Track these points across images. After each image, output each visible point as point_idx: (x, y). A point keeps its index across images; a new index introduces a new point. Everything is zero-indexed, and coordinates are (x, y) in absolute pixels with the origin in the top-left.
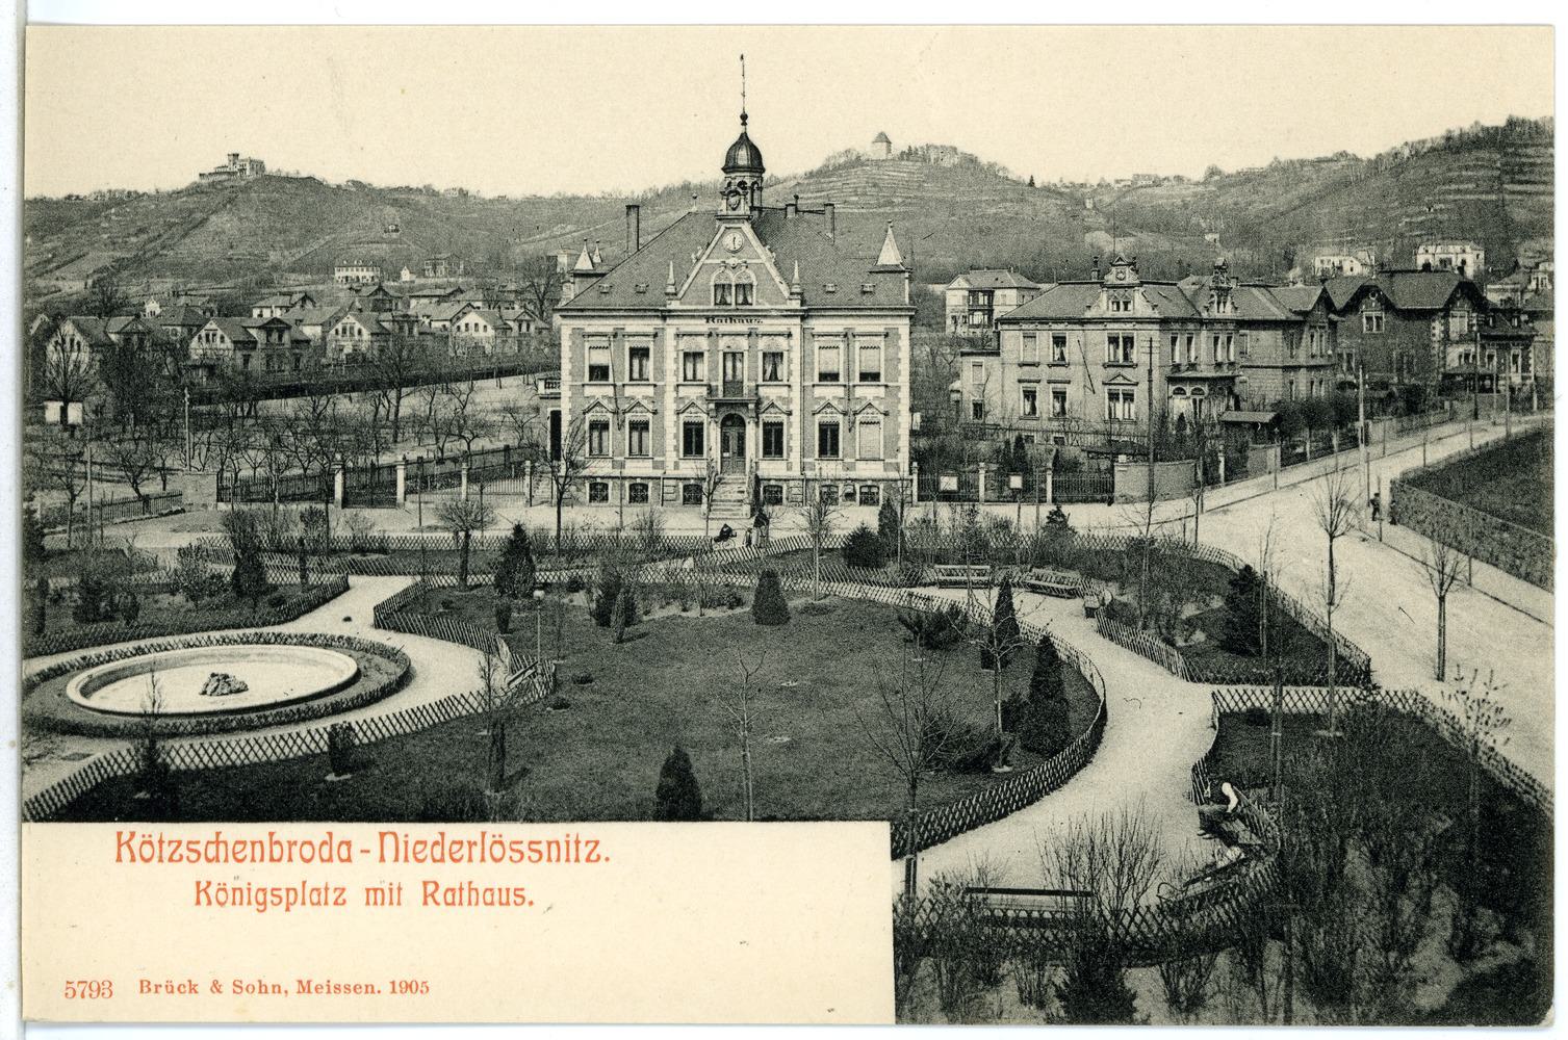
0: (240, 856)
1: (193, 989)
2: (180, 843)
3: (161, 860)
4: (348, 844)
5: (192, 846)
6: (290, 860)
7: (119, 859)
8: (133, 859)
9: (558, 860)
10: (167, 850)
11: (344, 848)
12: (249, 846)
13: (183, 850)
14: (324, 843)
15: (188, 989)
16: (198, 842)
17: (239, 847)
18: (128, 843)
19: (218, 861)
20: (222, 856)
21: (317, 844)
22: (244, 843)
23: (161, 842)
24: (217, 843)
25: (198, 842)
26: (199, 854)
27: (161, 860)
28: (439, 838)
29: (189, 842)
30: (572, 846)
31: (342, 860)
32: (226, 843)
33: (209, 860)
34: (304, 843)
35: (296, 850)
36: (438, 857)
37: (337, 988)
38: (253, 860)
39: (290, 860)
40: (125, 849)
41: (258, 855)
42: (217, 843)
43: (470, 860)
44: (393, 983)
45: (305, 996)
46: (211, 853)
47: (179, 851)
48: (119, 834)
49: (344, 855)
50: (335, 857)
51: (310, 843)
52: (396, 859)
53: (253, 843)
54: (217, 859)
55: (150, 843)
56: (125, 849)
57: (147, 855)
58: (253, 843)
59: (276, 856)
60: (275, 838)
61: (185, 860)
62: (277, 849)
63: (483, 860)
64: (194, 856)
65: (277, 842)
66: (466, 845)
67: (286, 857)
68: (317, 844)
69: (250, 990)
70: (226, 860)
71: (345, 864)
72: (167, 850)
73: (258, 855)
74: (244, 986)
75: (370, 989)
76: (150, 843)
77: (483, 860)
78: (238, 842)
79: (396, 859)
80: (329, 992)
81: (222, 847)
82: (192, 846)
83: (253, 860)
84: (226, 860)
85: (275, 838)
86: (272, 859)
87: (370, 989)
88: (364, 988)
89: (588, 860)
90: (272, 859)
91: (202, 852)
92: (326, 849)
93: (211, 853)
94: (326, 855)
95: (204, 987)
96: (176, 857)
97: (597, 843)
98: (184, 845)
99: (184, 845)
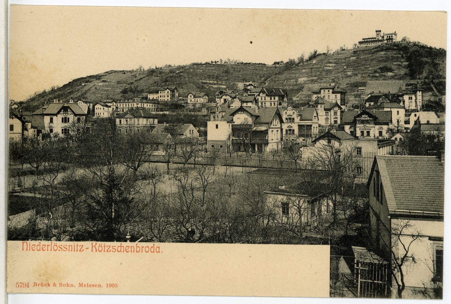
0: (127, 251)
1: (49, 285)
2: (110, 246)
3: (104, 251)
4: (159, 247)
5: (113, 247)
6: (142, 252)
7: (92, 251)
8: (96, 251)
9: (72, 251)
10: (106, 249)
11: (158, 249)
12: (130, 247)
13: (111, 248)
14: (152, 247)
15: (47, 285)
16: (115, 246)
17: (127, 248)
18: (95, 246)
19: (121, 252)
20: (122, 250)
21: (150, 247)
24: (121, 247)
25: (115, 246)
26: (67, 249)
27: (104, 251)
28: (153, 246)
29: (113, 246)
30: (76, 247)
31: (157, 252)
32: (123, 247)
33: (118, 252)
34: (146, 247)
35: (144, 249)
36: (152, 251)
37: (90, 286)
38: (131, 252)
39: (142, 252)
40: (94, 248)
41: (133, 251)
42: (121, 247)
43: (48, 250)
44: (107, 284)
45: (81, 288)
46: (119, 249)
47: (110, 249)
48: (92, 244)
49: (158, 250)
50: (155, 251)
52: (27, 250)
53: (131, 247)
55: (101, 246)
56: (94, 248)
57: (100, 250)
58: (131, 247)
60: (138, 246)
61: (111, 251)
62: (138, 249)
63: (51, 250)
64: (114, 250)
65: (139, 247)
66: (46, 246)
68: (150, 247)
69: (64, 285)
70: (123, 252)
71: (152, 253)
72: (106, 249)
73: (133, 251)
74: (63, 284)
75: (100, 286)
76: (101, 246)
77: (51, 250)
78: (127, 247)
79: (27, 250)
80: (88, 287)
81: (122, 248)
82: (113, 247)
83: (131, 252)
84: (123, 252)
85: (138, 246)
86: (137, 252)
87: (100, 286)
88: (98, 286)
89: (107, 251)
90: (137, 252)
91: (117, 250)
92: (152, 249)
93: (119, 249)
94: (152, 251)
95: (31, 284)
96: (109, 250)
97: (83, 246)
98: (111, 247)
99: (111, 247)
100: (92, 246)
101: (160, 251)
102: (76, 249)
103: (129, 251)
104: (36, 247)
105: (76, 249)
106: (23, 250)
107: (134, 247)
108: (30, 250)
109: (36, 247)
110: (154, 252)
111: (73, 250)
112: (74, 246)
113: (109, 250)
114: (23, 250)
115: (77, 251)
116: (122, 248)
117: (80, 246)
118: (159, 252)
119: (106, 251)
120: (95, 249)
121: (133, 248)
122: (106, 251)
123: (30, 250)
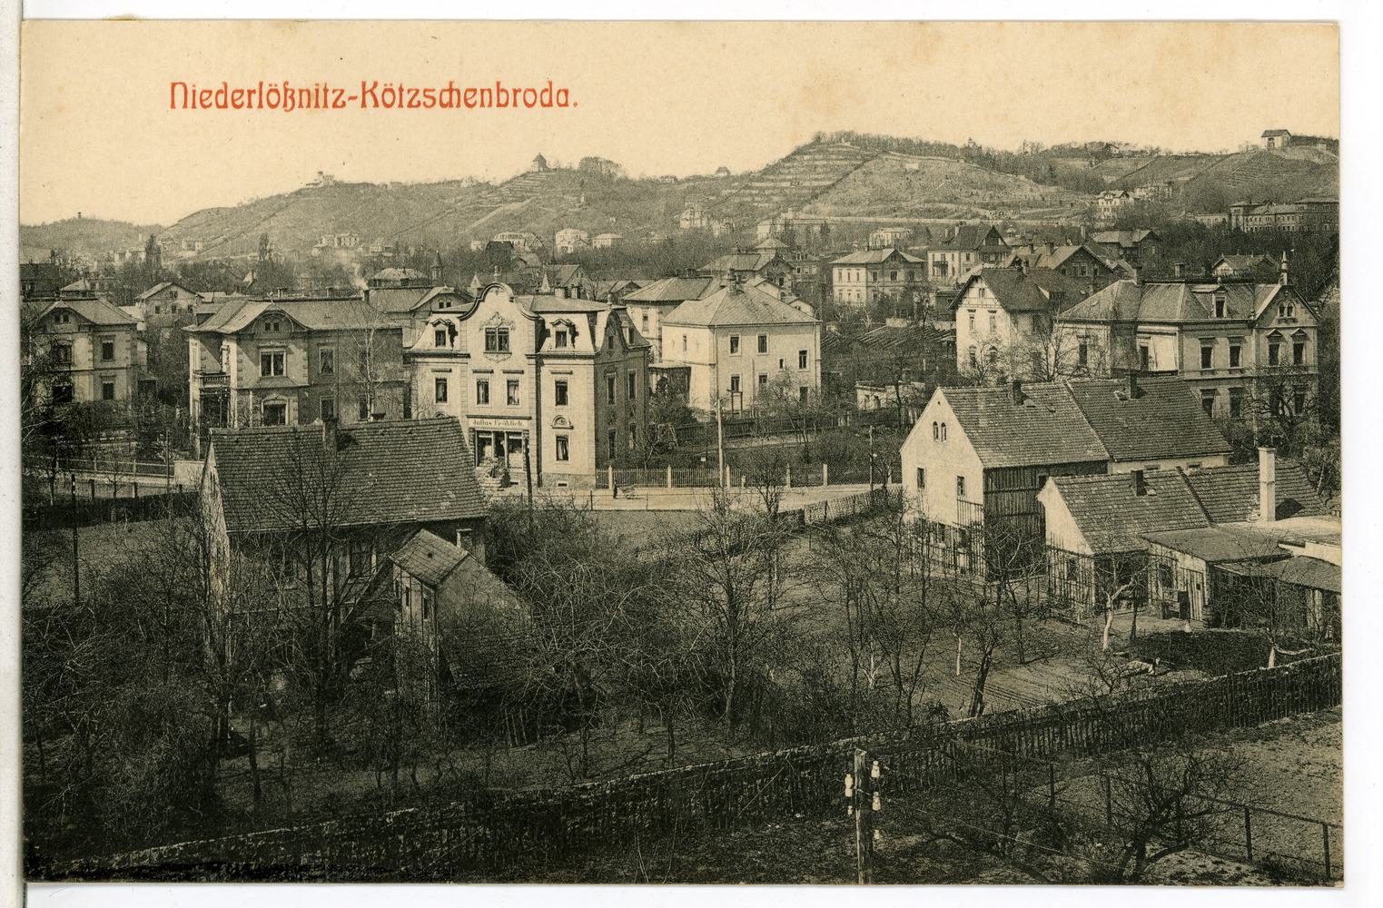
2: (417, 91)
3: (401, 105)
4: (566, 92)
5: (427, 93)
6: (515, 104)
7: (364, 105)
8: (376, 105)
11: (562, 95)
13: (420, 97)
14: (546, 90)
16: (433, 90)
18: (371, 91)
19: (451, 106)
21: (539, 92)
22: (475, 91)
23: (401, 90)
25: (433, 90)
27: (401, 105)
29: (425, 91)
31: (560, 105)
33: (442, 105)
35: (519, 96)
38: (482, 105)
39: (515, 104)
42: (451, 90)
46: (446, 99)
47: (417, 98)
51: (534, 91)
54: (450, 104)
57: (389, 101)
58: (482, 91)
59: (503, 101)
61: (422, 106)
64: (429, 102)
65: (503, 90)
67: (511, 101)
68: (539, 92)
70: (458, 106)
77: (260, 106)
81: (455, 94)
82: (427, 93)
83: (482, 105)
86: (499, 105)
94: (546, 101)
96: (414, 103)
97: (342, 91)
98: (421, 93)
99: (421, 93)
100: (364, 88)
101: (571, 102)
102: (321, 103)
103: (475, 104)
104: (212, 99)
105: (321, 103)
106: (173, 106)
107: (490, 90)
108: (194, 107)
109: (212, 99)
110: (550, 104)
111: (313, 103)
112: (317, 91)
113: (414, 103)
114: (173, 106)
115: (326, 105)
116: (455, 94)
117: (334, 91)
118: (566, 105)
119: (405, 102)
120: (372, 98)
121: (486, 95)
122: (405, 102)
123: (194, 107)
